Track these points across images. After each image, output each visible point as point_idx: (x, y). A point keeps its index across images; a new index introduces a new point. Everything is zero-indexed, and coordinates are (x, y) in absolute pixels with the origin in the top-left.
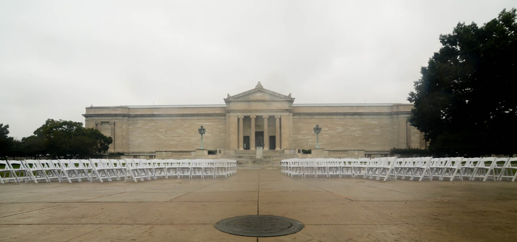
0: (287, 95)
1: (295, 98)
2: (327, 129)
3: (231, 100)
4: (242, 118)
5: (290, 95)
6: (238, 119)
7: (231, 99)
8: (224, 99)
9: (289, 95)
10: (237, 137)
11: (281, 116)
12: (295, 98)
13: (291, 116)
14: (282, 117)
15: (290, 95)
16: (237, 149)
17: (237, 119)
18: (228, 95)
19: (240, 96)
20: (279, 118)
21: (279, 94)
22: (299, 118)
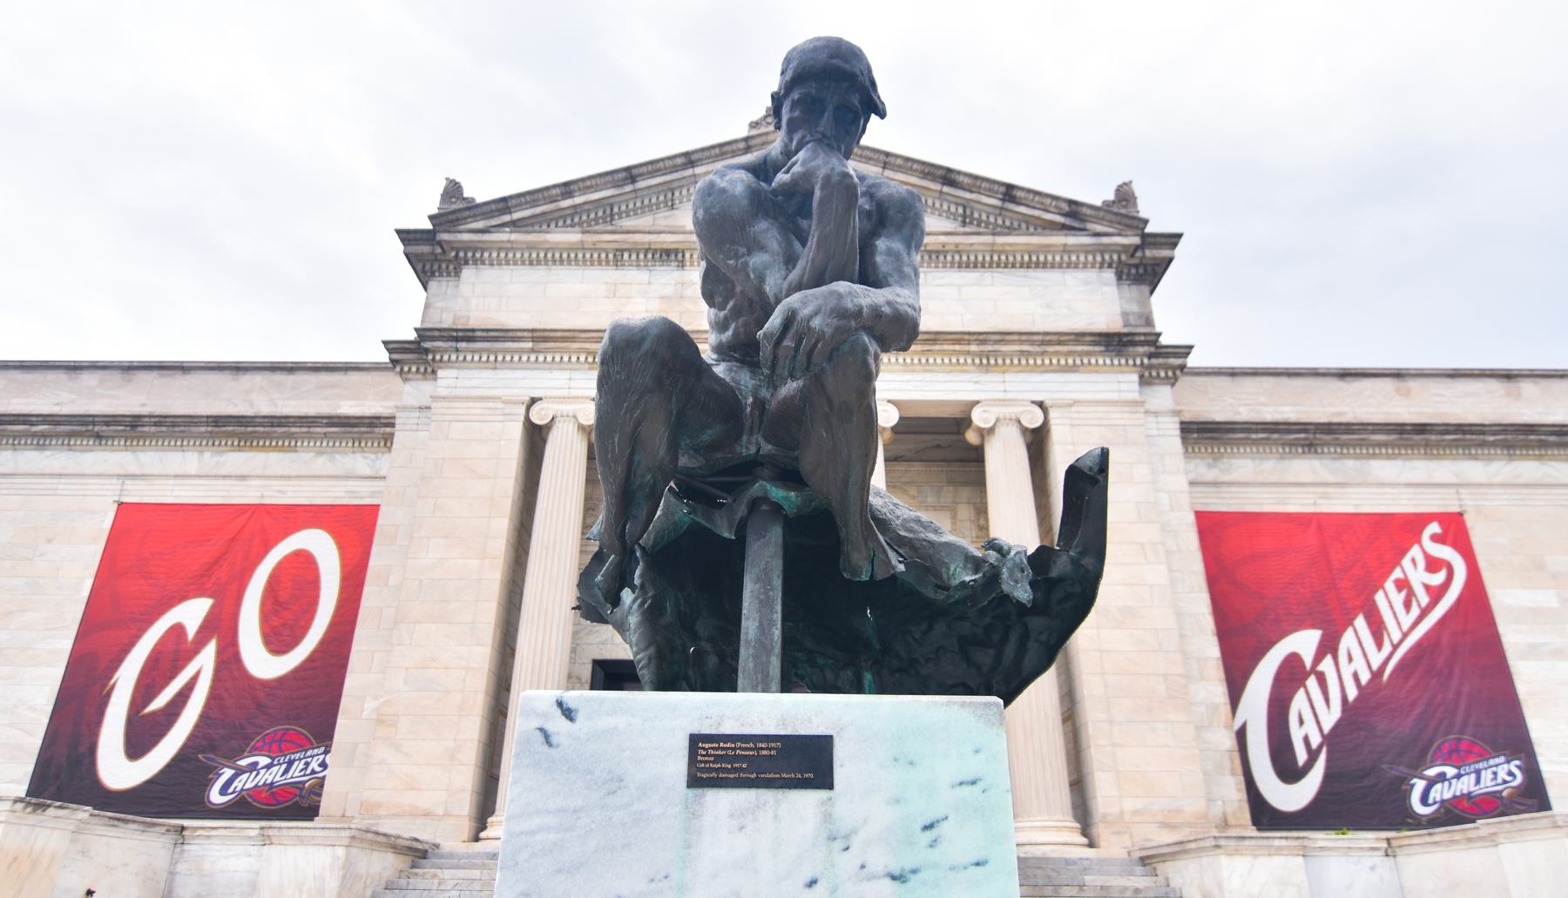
0: (1098, 203)
1: (1179, 236)
2: (1547, 598)
3: (466, 237)
4: (581, 428)
5: (1125, 195)
6: (536, 437)
7: (480, 225)
8: (406, 236)
9: (1111, 197)
10: (482, 655)
11: (1041, 405)
12: (1179, 236)
13: (1156, 414)
14: (1053, 414)
15: (1125, 195)
16: (466, 826)
17: (516, 431)
18: (453, 190)
19: (579, 200)
20: (1025, 431)
21: (1009, 192)
22: (1216, 484)
